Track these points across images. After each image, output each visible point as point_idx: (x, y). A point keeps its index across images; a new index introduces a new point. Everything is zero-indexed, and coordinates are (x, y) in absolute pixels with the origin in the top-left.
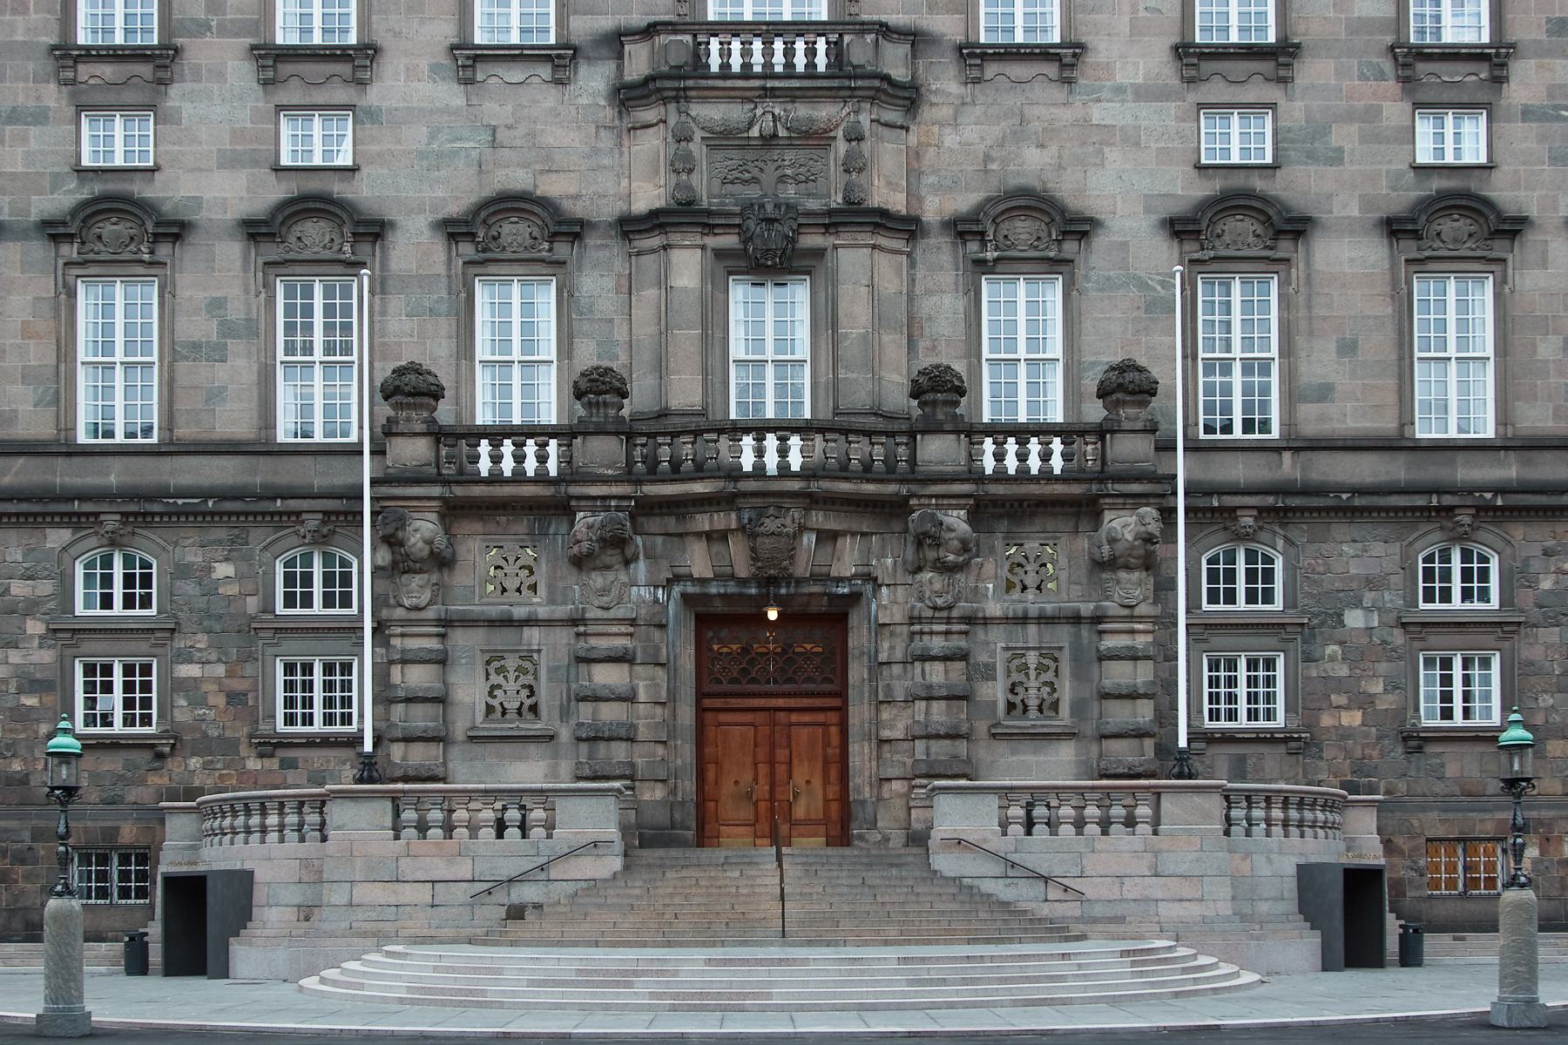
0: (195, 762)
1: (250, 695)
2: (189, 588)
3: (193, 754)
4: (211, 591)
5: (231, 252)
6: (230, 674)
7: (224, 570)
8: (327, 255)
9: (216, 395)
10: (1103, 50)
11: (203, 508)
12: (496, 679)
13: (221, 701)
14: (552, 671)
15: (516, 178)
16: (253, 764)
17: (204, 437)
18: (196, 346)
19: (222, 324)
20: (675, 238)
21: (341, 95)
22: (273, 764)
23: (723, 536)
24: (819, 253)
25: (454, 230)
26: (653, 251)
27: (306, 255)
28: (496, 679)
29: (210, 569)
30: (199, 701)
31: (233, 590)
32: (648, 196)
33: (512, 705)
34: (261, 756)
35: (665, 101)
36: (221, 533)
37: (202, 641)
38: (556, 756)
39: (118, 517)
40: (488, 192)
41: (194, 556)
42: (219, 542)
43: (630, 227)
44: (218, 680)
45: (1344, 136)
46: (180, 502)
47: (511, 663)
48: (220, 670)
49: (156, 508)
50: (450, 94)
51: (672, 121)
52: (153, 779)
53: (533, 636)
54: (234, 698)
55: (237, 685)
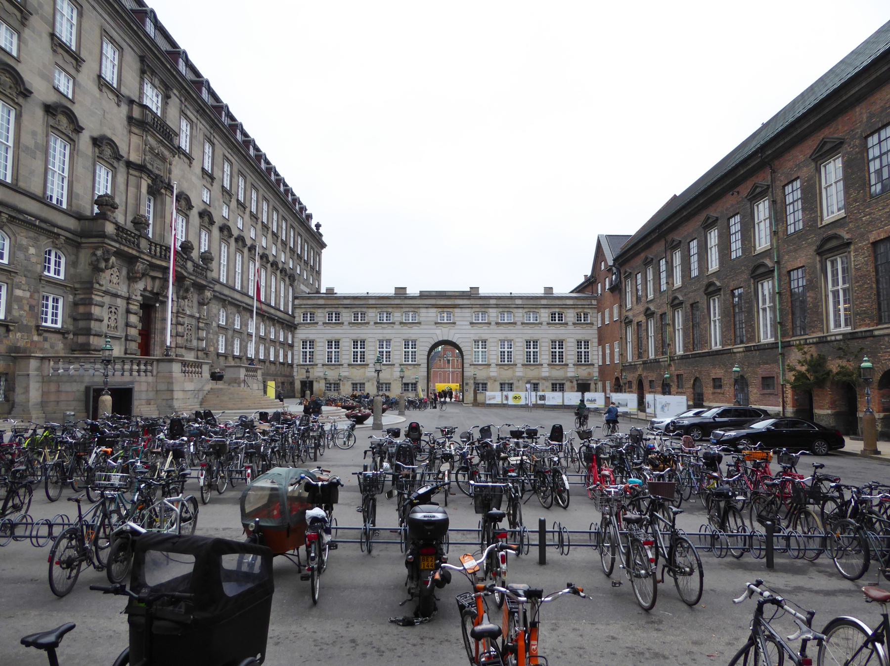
0: (19, 335)
1: (36, 308)
2: (20, 255)
3: (19, 331)
4: (27, 259)
5: (40, 113)
6: (31, 297)
7: (32, 250)
8: (64, 131)
9: (32, 172)
10: (194, 163)
11: (34, 223)
12: (110, 316)
13: (27, 308)
14: (122, 314)
15: (109, 134)
16: (36, 338)
17: (27, 189)
18: (27, 148)
19: (36, 143)
20: (143, 176)
21: (72, 71)
22: (41, 339)
23: (154, 278)
24: (161, 194)
25: (97, 142)
26: (136, 176)
27: (59, 128)
28: (110, 316)
29: (27, 249)
30: (21, 308)
31: (34, 260)
32: (134, 157)
33: (113, 325)
34: (39, 335)
35: (144, 130)
36: (32, 234)
37: (23, 280)
38: (121, 345)
39: (7, 216)
40: (102, 133)
41: (24, 242)
42: (30, 237)
43: (129, 164)
44: (27, 299)
45: (216, 204)
46: (29, 218)
47: (113, 310)
48: (28, 294)
49: (21, 217)
50: (94, 89)
51: (144, 138)
52: (5, 341)
53: (119, 301)
54: (32, 308)
55: (34, 303)
